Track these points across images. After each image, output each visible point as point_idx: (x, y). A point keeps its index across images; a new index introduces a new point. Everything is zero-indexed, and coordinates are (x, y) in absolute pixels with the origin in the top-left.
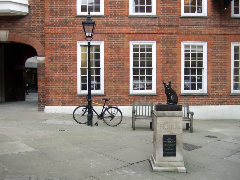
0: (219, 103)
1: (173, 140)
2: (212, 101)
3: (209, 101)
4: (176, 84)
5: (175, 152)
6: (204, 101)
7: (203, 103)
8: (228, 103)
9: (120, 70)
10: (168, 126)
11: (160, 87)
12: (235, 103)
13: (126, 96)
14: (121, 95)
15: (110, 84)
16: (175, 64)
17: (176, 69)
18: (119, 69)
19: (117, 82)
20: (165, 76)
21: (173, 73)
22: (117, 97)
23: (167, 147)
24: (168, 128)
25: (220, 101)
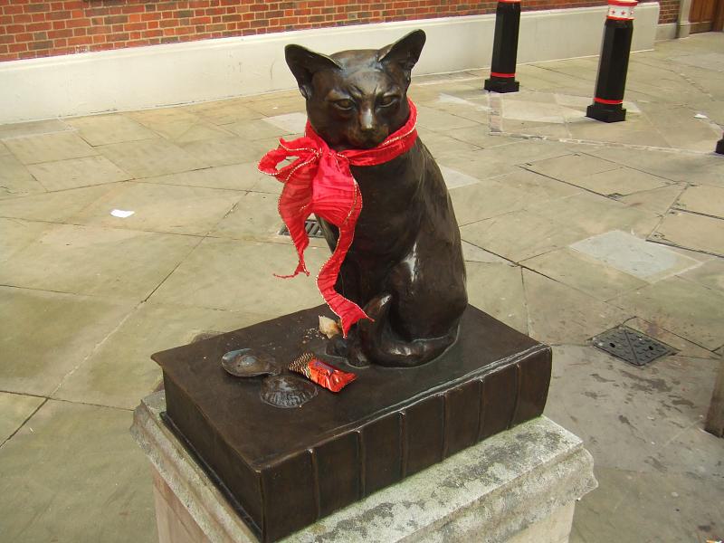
0: (255, 24)
2: (226, 19)
3: (215, 20)
6: (195, 22)
7: (191, 30)
8: (288, 21)
12: (312, 19)
25: (258, 16)
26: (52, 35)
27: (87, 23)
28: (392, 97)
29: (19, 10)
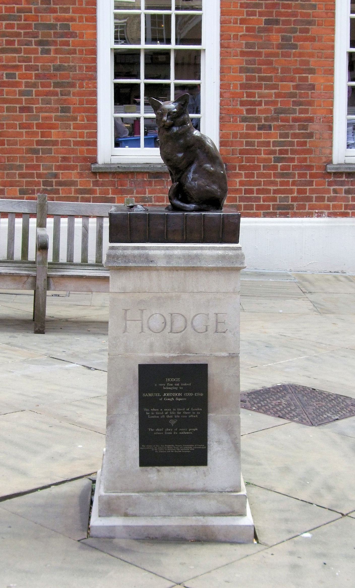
1: (187, 389)
4: (311, 120)
5: (201, 447)
9: (52, 55)
10: (168, 319)
11: (235, 135)
13: (81, 175)
14: (59, 168)
15: (7, 118)
16: (307, 31)
17: (312, 55)
18: (48, 52)
19: (40, 110)
20: (259, 87)
21: (297, 71)
22: (39, 176)
23: (164, 423)
24: (168, 328)
26: (294, 199)
27: (328, 192)
28: (174, 112)
29: (269, 176)
